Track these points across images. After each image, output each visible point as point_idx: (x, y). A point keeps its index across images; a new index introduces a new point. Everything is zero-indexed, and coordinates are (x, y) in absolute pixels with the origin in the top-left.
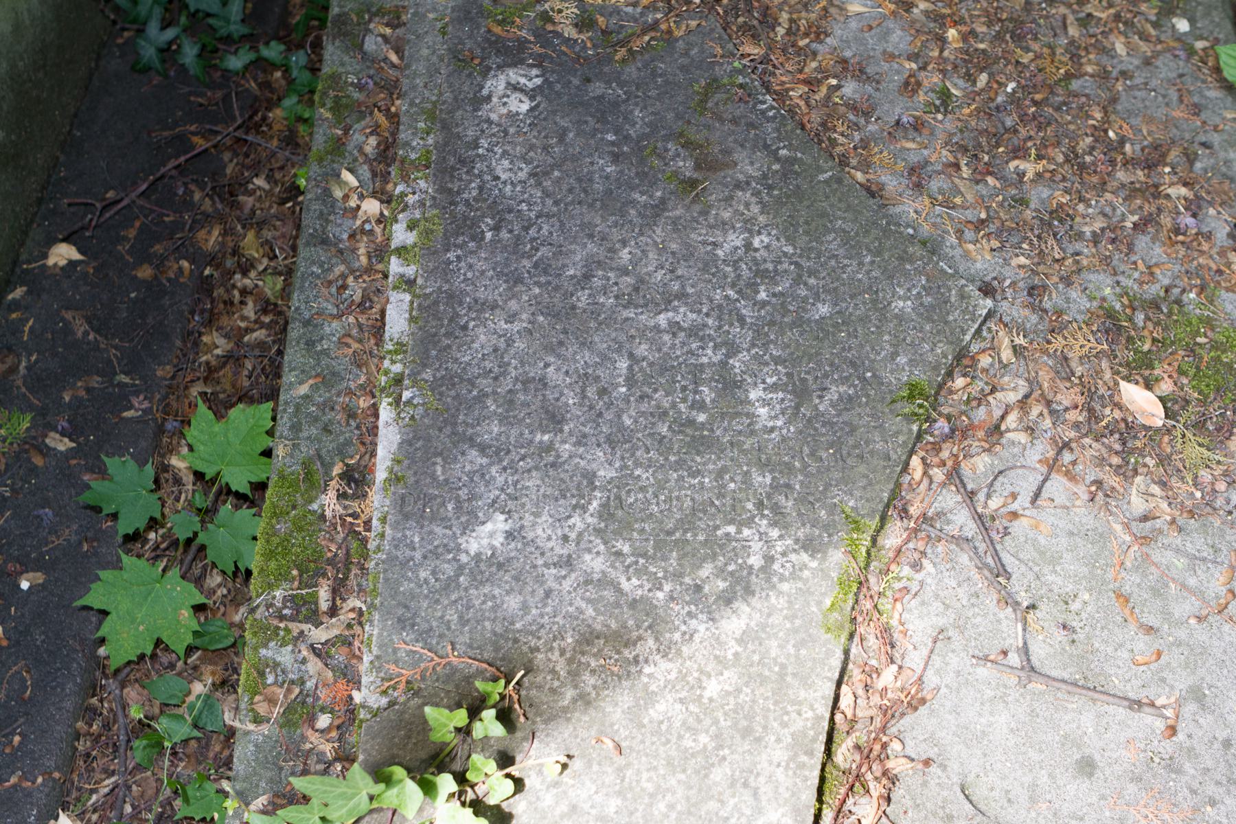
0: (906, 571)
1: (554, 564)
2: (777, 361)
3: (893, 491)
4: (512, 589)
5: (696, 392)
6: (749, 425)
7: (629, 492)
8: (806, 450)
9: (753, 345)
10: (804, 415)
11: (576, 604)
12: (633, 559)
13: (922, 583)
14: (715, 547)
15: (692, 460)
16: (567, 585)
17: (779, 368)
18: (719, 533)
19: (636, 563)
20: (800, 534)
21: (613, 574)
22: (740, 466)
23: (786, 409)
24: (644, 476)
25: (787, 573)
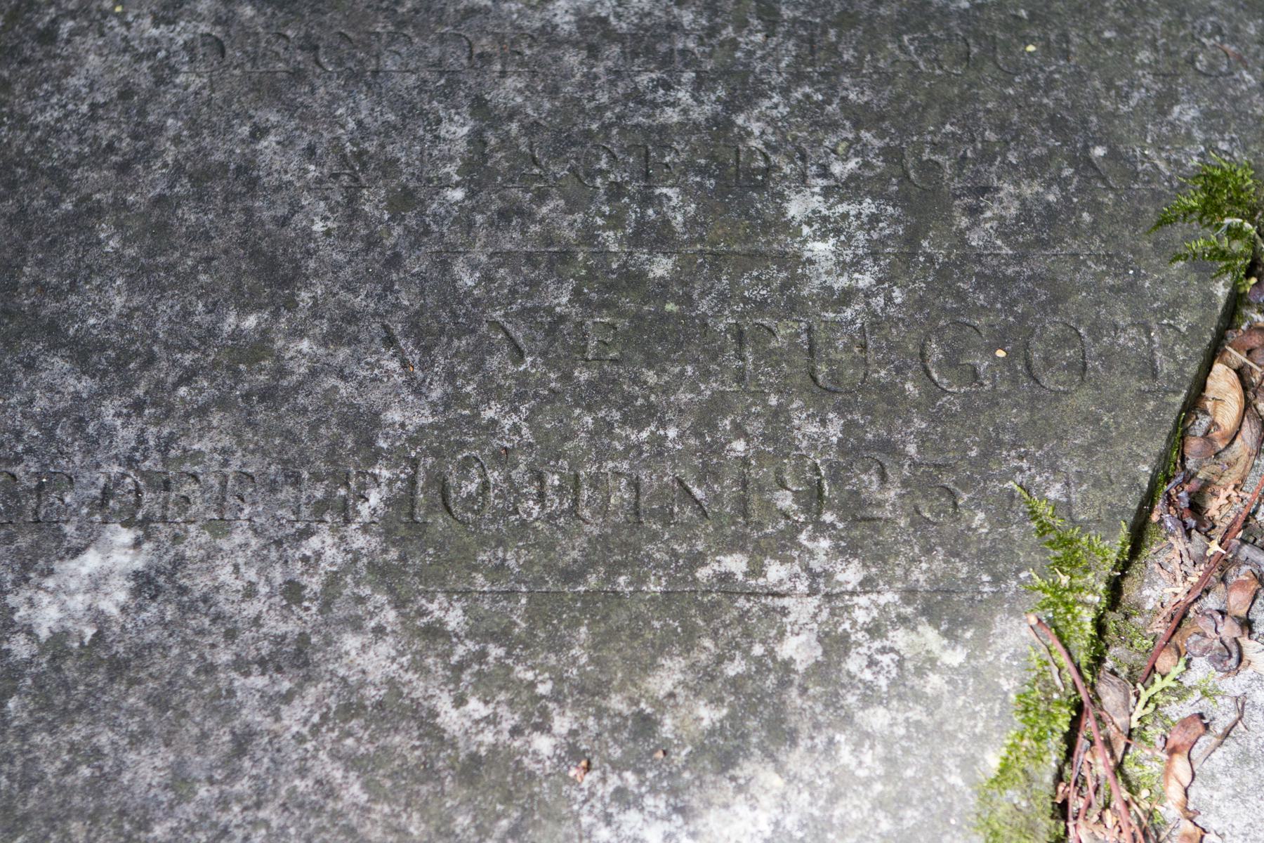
0: (1202, 670)
1: (262, 663)
2: (859, 117)
3: (1164, 458)
4: (146, 732)
5: (647, 199)
6: (784, 286)
7: (466, 464)
8: (935, 351)
9: (798, 77)
10: (930, 259)
11: (318, 771)
12: (471, 645)
13: (1241, 704)
14: (697, 611)
15: (636, 380)
16: (293, 718)
17: (866, 135)
18: (703, 573)
19: (482, 656)
20: (919, 575)
21: (417, 686)
22: (761, 395)
23: (883, 242)
24: (507, 423)
25: (883, 682)
